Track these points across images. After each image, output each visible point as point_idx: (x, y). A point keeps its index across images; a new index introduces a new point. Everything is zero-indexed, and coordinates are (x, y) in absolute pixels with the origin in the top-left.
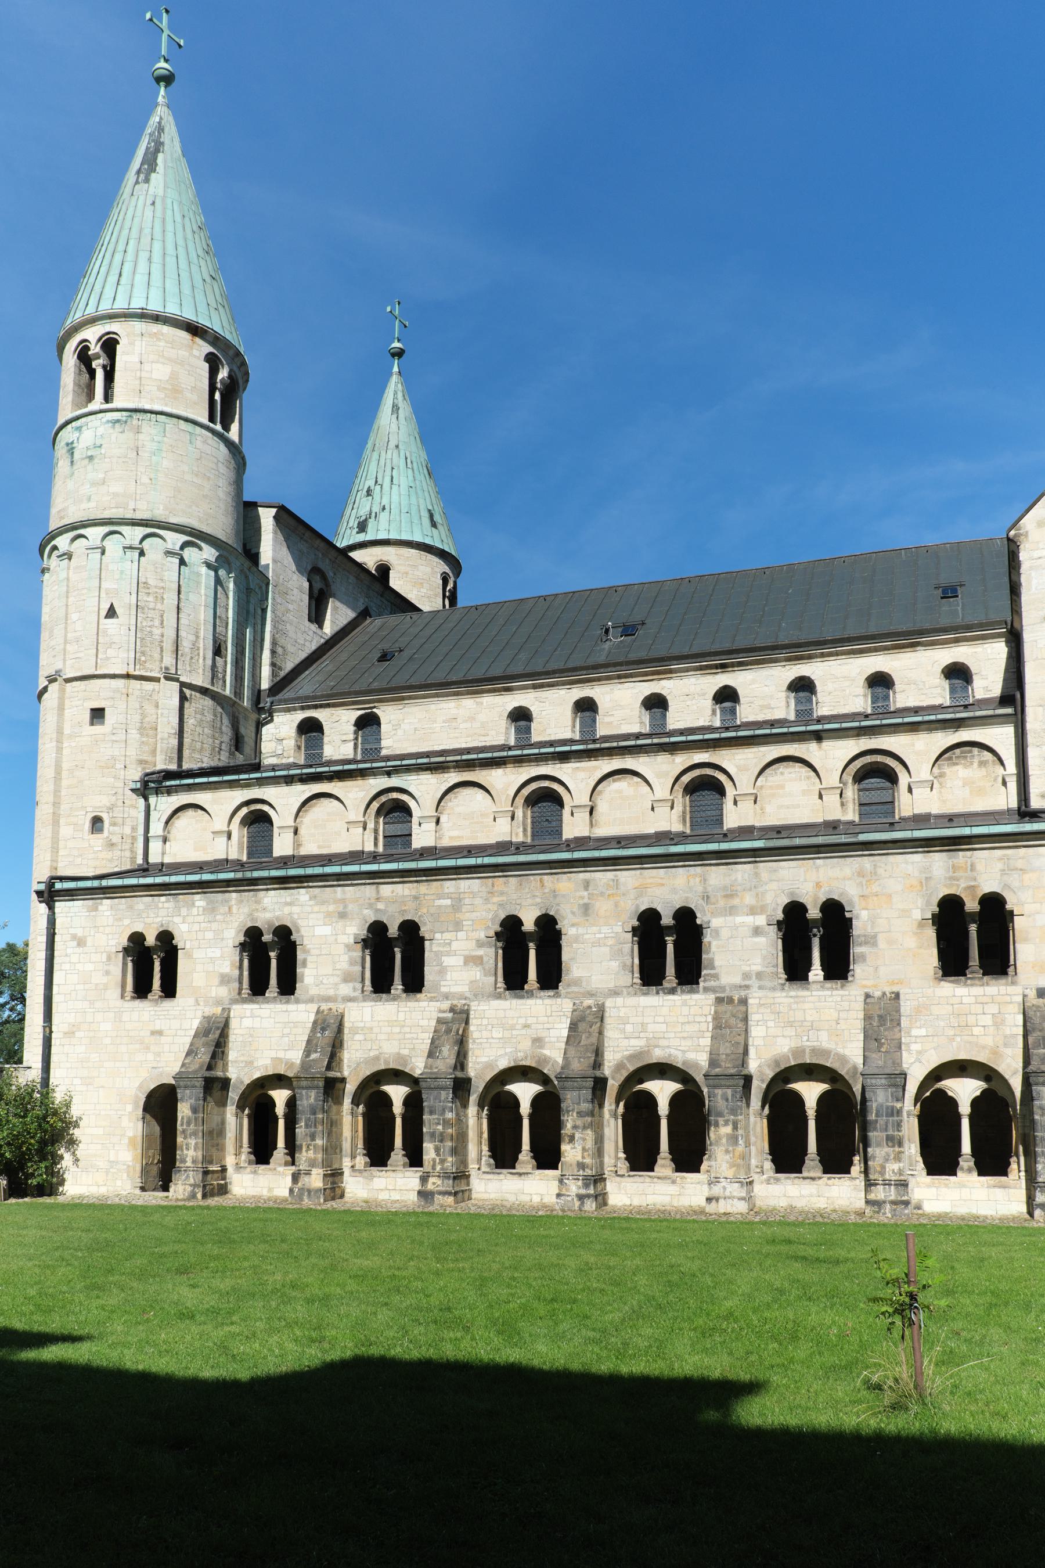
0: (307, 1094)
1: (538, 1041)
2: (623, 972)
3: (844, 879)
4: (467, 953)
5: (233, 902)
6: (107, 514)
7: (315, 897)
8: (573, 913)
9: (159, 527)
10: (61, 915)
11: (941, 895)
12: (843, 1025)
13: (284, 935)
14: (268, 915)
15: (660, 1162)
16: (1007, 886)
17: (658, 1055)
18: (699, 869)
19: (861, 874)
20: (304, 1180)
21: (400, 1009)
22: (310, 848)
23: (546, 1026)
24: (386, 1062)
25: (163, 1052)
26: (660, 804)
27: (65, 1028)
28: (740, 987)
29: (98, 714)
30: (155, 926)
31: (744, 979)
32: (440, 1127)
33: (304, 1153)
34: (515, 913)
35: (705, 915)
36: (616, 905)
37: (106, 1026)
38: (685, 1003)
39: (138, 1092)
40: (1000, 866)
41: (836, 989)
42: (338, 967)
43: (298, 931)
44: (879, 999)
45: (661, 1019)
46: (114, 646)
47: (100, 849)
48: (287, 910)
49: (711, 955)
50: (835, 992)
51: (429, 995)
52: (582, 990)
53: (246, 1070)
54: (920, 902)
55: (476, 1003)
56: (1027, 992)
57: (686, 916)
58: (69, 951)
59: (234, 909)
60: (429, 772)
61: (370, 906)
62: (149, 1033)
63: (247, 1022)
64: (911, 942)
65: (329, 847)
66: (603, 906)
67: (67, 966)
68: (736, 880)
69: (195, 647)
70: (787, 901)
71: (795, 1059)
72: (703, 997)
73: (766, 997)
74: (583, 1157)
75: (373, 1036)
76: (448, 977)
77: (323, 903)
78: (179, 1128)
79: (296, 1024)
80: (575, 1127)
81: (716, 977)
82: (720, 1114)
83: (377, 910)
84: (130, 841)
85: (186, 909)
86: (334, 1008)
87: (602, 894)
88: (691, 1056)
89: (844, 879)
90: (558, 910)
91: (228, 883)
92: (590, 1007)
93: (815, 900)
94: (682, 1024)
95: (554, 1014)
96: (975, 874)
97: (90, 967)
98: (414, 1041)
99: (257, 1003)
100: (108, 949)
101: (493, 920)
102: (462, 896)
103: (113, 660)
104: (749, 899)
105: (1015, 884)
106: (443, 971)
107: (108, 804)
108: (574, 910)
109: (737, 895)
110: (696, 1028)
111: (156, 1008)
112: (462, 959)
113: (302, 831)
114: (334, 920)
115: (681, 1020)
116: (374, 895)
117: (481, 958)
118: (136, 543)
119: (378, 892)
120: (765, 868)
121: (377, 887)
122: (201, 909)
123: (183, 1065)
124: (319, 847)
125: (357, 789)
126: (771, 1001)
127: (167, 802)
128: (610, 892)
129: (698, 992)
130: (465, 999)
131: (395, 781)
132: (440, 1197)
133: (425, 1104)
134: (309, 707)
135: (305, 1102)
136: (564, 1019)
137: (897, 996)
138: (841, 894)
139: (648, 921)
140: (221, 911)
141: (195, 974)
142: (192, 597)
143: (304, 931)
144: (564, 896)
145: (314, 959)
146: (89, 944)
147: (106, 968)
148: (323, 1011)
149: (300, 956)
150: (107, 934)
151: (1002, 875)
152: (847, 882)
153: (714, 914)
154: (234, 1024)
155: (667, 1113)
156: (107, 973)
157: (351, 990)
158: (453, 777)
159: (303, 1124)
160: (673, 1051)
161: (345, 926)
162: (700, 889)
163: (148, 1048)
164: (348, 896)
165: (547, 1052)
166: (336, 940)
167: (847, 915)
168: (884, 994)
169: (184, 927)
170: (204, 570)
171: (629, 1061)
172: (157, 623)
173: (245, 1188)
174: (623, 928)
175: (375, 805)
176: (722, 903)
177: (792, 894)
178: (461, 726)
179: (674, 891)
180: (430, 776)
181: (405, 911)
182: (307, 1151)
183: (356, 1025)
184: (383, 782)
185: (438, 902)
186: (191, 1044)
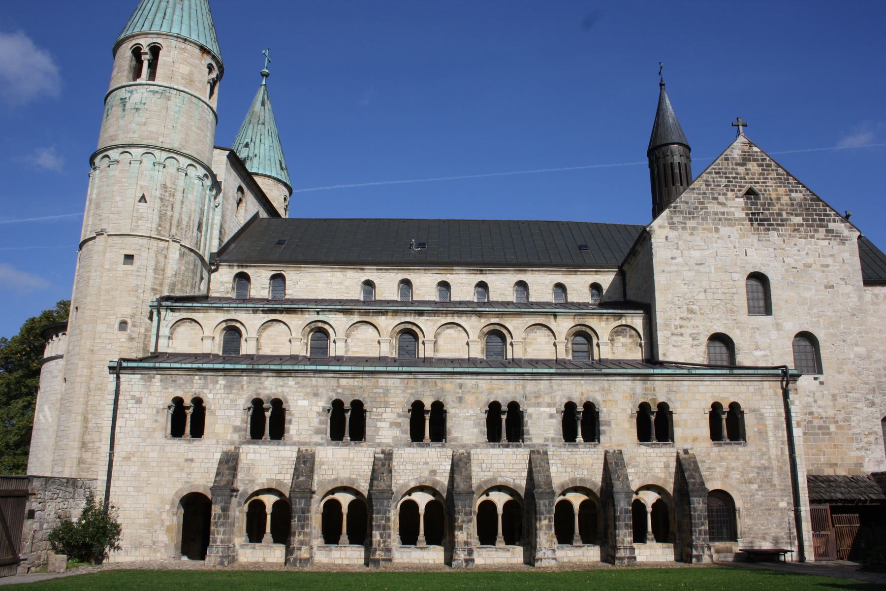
0: (299, 501)
1: (433, 472)
2: (480, 435)
3: (595, 391)
4: (392, 420)
5: (245, 383)
6: (145, 142)
7: (299, 383)
8: (453, 401)
9: (177, 153)
10: (125, 383)
11: (640, 402)
12: (595, 467)
13: (278, 406)
14: (267, 392)
15: (498, 539)
16: (669, 399)
17: (500, 481)
18: (521, 382)
19: (603, 389)
20: (297, 554)
22: (266, 351)
23: (437, 463)
24: (342, 482)
25: (193, 473)
26: (473, 343)
27: (124, 454)
28: (543, 445)
29: (129, 258)
30: (191, 394)
31: (545, 441)
32: (383, 522)
33: (297, 537)
34: (420, 399)
35: (524, 406)
36: (477, 398)
37: (154, 455)
39: (174, 497)
40: (666, 389)
41: (592, 448)
42: (312, 425)
43: (287, 402)
44: (613, 453)
45: (502, 462)
46: (142, 219)
47: (124, 340)
48: (280, 389)
49: (527, 428)
50: (591, 450)
51: (368, 443)
52: (458, 444)
53: (250, 485)
54: (630, 405)
55: (397, 449)
56: (679, 451)
57: (514, 406)
58: (129, 406)
59: (245, 387)
60: (342, 314)
61: (333, 390)
62: (183, 460)
63: (251, 456)
64: (626, 425)
65: (278, 351)
66: (469, 399)
67: (127, 416)
68: (541, 389)
69: (188, 225)
70: (566, 401)
71: (572, 483)
72: (523, 450)
73: (556, 451)
74: (467, 538)
75: (334, 467)
76: (380, 434)
77: (303, 386)
78: (212, 520)
79: (283, 458)
80: (463, 521)
81: (530, 439)
82: (543, 514)
83: (337, 393)
84: (143, 337)
85: (212, 385)
86: (309, 449)
87: (469, 392)
88: (517, 482)
89: (595, 391)
90: (444, 400)
91: (243, 370)
92: (463, 454)
93: (581, 401)
94: (513, 464)
95: (442, 457)
96: (655, 392)
97: (143, 417)
98: (359, 470)
99: (258, 444)
100: (157, 406)
101: (407, 403)
102: (389, 388)
103: (141, 227)
104: (547, 399)
105: (673, 398)
106: (377, 429)
107: (131, 313)
109: (541, 397)
110: (520, 466)
111: (189, 445)
112: (388, 423)
113: (262, 341)
114: (310, 397)
115: (513, 462)
116: (336, 384)
117: (400, 423)
118: (162, 161)
119: (338, 383)
120: (557, 381)
121: (338, 380)
122: (222, 386)
123: (215, 482)
124: (271, 351)
125: (298, 319)
126: (559, 453)
127: (173, 316)
128: (474, 391)
130: (390, 446)
131: (321, 317)
132: (383, 562)
133: (374, 508)
134: (242, 266)
135: (298, 506)
136: (447, 460)
137: (621, 452)
138: (594, 399)
139: (494, 409)
140: (236, 387)
141: (217, 425)
142: (190, 196)
143: (290, 403)
144: (448, 391)
145: (297, 419)
147: (155, 418)
148: (302, 451)
149: (287, 417)
150: (157, 397)
151: (667, 394)
152: (597, 393)
154: (242, 457)
155: (502, 513)
156: (156, 421)
157: (320, 438)
158: (356, 318)
159: (296, 519)
160: (508, 479)
161: (317, 401)
162: (522, 392)
163: (182, 469)
164: (320, 384)
165: (438, 478)
166: (311, 409)
167: (597, 410)
168: (615, 451)
169: (210, 396)
170: (197, 181)
171: (484, 484)
172: (170, 208)
173: (247, 558)
174: (481, 411)
175: (308, 329)
176: (533, 400)
177: (569, 398)
178: (334, 287)
179: (508, 392)
180: (342, 316)
181: (355, 394)
182: (299, 536)
183: (323, 459)
184: (313, 317)
185: (375, 391)
186: (218, 469)
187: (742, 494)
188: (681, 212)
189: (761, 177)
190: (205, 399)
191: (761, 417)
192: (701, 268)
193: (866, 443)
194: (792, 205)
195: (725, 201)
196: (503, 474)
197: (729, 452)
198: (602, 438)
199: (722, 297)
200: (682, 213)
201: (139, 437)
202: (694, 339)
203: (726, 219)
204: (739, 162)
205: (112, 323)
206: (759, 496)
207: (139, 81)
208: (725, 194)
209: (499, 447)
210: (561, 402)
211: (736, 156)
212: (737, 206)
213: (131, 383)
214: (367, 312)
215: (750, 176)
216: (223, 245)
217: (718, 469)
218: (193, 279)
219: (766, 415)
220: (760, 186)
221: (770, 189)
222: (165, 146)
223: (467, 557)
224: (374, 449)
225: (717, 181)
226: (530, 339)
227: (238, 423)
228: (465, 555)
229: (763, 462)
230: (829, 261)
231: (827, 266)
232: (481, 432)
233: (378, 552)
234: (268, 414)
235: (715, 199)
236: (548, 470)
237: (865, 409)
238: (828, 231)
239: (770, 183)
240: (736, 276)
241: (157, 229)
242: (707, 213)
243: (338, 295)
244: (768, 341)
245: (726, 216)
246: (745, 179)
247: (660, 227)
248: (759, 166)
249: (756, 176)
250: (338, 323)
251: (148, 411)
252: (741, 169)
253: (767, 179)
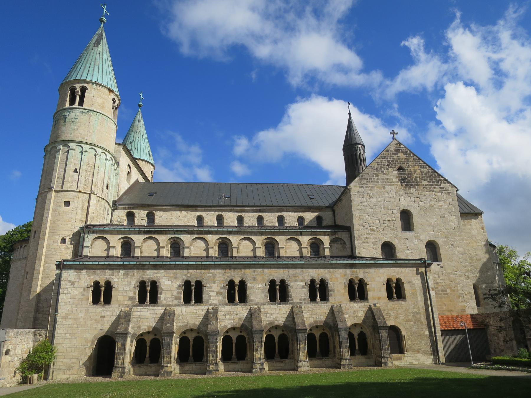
4: (217, 291)
8: (251, 280)
9: (95, 146)
14: (148, 277)
16: (365, 277)
21: (195, 309)
24: (190, 326)
27: (64, 315)
30: (104, 279)
32: (214, 348)
34: (233, 279)
36: (263, 278)
37: (81, 314)
38: (284, 307)
42: (173, 294)
43: (159, 282)
45: (277, 312)
47: (63, 249)
48: (155, 275)
50: (325, 305)
54: (345, 281)
56: (371, 305)
57: (283, 282)
58: (67, 287)
59: (135, 274)
61: (185, 275)
63: (138, 313)
64: (343, 291)
66: (259, 278)
68: (297, 272)
70: (311, 279)
72: (289, 306)
73: (306, 306)
80: (258, 347)
81: (292, 300)
86: (172, 308)
87: (259, 274)
90: (246, 279)
92: (256, 308)
93: (318, 278)
96: (357, 273)
97: (76, 293)
99: (142, 307)
100: (84, 286)
101: (226, 281)
104: (301, 278)
105: (367, 276)
106: (210, 296)
107: (68, 234)
108: (251, 279)
111: (102, 308)
117: (222, 293)
129: (287, 304)
130: (217, 305)
138: (325, 277)
139: (272, 283)
144: (248, 274)
146: (76, 284)
147: (83, 293)
149: (159, 291)
152: (326, 274)
153: (291, 281)
156: (83, 295)
163: (99, 322)
169: (115, 280)
176: (293, 279)
177: (312, 277)
182: (166, 358)
185: (209, 275)
187: (406, 327)
188: (365, 179)
189: (406, 160)
190: (112, 282)
191: (413, 286)
193: (466, 298)
194: (422, 174)
195: (387, 173)
196: (278, 319)
197: (397, 304)
198: (330, 298)
199: (388, 222)
200: (366, 179)
201: (73, 304)
202: (374, 245)
203: (389, 182)
204: (394, 152)
205: (56, 239)
206: (414, 329)
207: (74, 106)
208: (387, 169)
209: (276, 304)
210: (308, 279)
211: (392, 150)
212: (393, 175)
213: (69, 273)
214: (201, 233)
215: (400, 160)
216: (119, 196)
217: (392, 314)
218: (103, 214)
219: (416, 284)
220: (405, 165)
221: (411, 166)
222: (88, 142)
223: (261, 367)
224: (208, 307)
225: (383, 163)
226: (288, 246)
227: (131, 294)
228: (259, 366)
229: (415, 310)
230: (442, 203)
231: (442, 206)
232: (266, 296)
233: (211, 366)
234: (148, 289)
236: (303, 317)
237: (465, 280)
238: (441, 188)
239: (410, 163)
240: (395, 212)
241: (84, 187)
242: (378, 179)
243: (184, 223)
244: (413, 245)
245: (388, 181)
246: (398, 161)
247: (355, 186)
248: (404, 154)
249: (403, 160)
250: (186, 239)
251: (78, 289)
253: (409, 161)
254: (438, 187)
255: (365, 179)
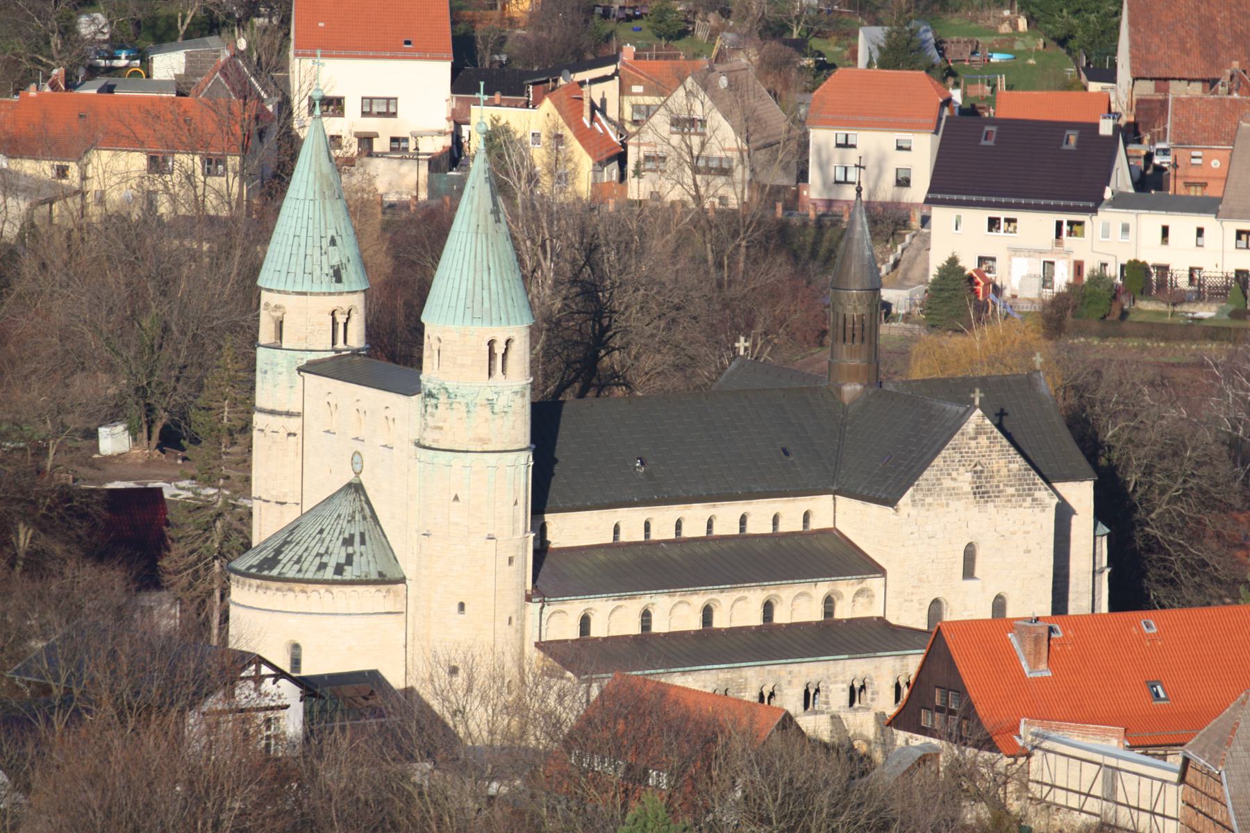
104: (841, 678)
188: (922, 490)
192: (933, 541)
194: (1009, 476)
202: (920, 604)
203: (956, 494)
208: (957, 470)
235: (949, 474)
238: (1034, 500)
239: (994, 455)
242: (941, 489)
249: (984, 449)
252: (973, 443)
253: (991, 451)
254: (1029, 499)
255: (922, 490)
